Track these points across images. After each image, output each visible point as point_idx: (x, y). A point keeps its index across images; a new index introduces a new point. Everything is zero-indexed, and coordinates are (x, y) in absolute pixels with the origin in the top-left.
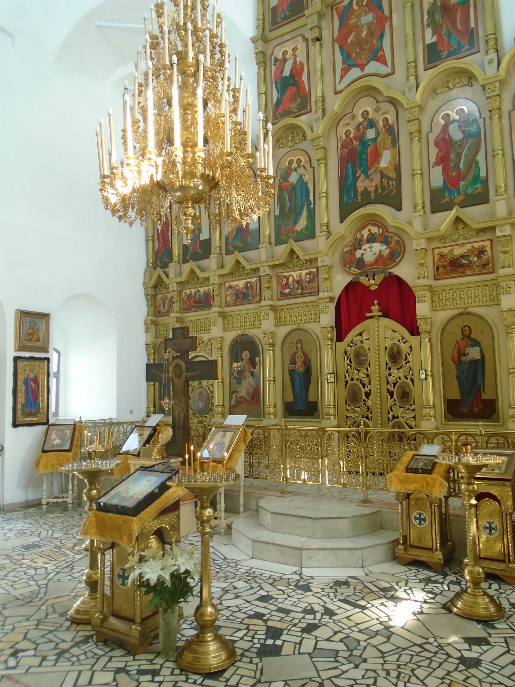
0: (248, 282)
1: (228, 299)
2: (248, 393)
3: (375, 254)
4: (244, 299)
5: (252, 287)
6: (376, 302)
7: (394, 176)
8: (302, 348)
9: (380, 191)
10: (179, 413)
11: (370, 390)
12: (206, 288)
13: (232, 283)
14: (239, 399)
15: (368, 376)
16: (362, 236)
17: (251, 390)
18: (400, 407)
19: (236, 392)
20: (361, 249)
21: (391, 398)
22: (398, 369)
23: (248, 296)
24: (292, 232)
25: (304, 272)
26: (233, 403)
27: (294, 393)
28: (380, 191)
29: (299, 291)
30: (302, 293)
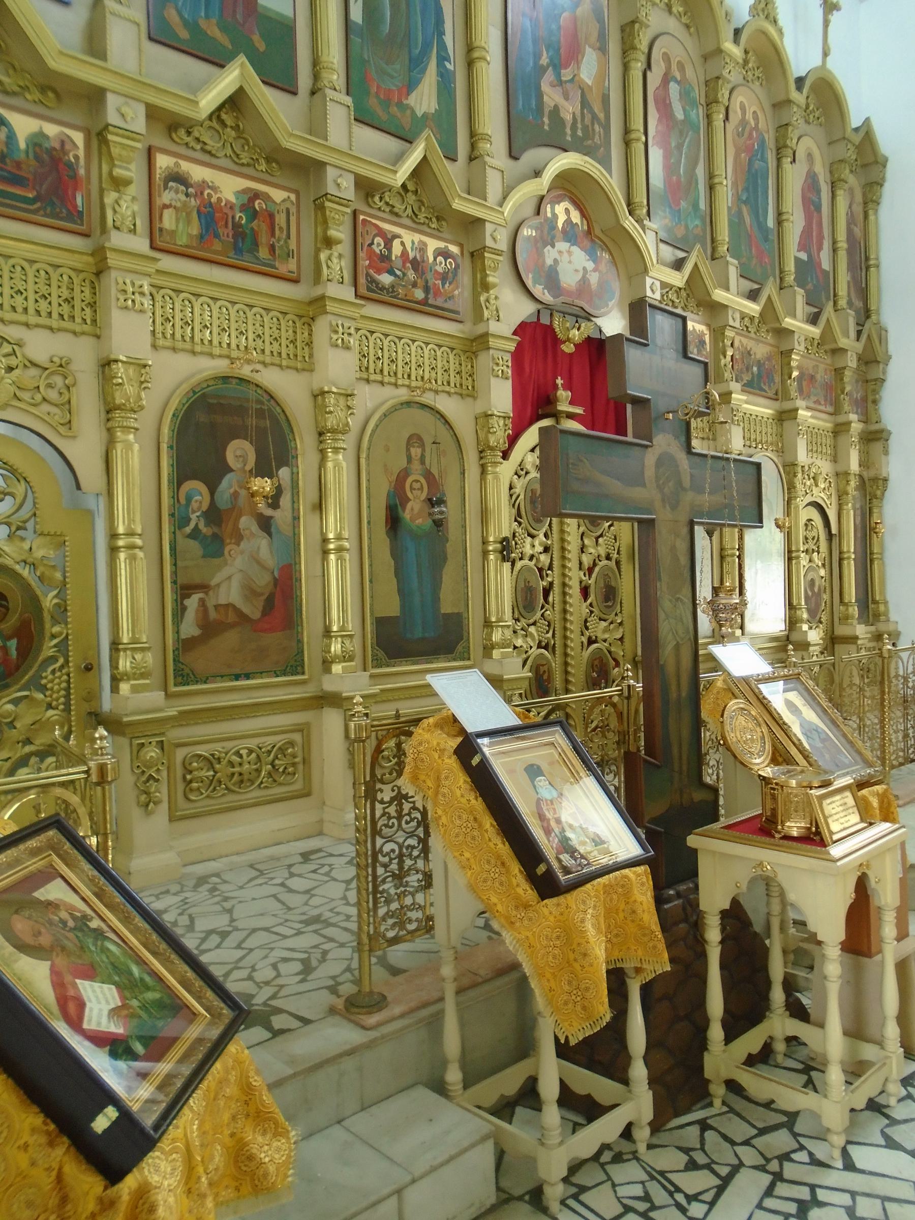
0: (256, 195)
1: (168, 220)
2: (250, 592)
3: (576, 271)
4: (238, 250)
5: (271, 216)
6: (559, 381)
7: (602, 116)
8: (422, 461)
9: (580, 133)
10: (677, 647)
11: (551, 584)
12: (51, 130)
13: (185, 166)
14: (213, 615)
15: (546, 550)
16: (555, 216)
17: (263, 581)
18: (600, 619)
19: (204, 587)
20: (553, 246)
21: (585, 601)
22: (597, 538)
23: (256, 244)
24: (400, 104)
25: (433, 245)
26: (189, 628)
27: (401, 592)
28: (580, 133)
29: (419, 294)
30: (425, 302)
